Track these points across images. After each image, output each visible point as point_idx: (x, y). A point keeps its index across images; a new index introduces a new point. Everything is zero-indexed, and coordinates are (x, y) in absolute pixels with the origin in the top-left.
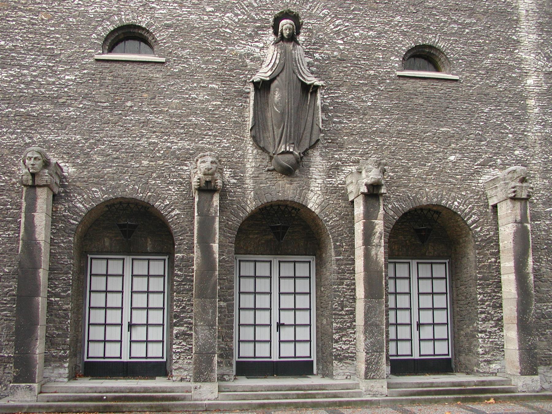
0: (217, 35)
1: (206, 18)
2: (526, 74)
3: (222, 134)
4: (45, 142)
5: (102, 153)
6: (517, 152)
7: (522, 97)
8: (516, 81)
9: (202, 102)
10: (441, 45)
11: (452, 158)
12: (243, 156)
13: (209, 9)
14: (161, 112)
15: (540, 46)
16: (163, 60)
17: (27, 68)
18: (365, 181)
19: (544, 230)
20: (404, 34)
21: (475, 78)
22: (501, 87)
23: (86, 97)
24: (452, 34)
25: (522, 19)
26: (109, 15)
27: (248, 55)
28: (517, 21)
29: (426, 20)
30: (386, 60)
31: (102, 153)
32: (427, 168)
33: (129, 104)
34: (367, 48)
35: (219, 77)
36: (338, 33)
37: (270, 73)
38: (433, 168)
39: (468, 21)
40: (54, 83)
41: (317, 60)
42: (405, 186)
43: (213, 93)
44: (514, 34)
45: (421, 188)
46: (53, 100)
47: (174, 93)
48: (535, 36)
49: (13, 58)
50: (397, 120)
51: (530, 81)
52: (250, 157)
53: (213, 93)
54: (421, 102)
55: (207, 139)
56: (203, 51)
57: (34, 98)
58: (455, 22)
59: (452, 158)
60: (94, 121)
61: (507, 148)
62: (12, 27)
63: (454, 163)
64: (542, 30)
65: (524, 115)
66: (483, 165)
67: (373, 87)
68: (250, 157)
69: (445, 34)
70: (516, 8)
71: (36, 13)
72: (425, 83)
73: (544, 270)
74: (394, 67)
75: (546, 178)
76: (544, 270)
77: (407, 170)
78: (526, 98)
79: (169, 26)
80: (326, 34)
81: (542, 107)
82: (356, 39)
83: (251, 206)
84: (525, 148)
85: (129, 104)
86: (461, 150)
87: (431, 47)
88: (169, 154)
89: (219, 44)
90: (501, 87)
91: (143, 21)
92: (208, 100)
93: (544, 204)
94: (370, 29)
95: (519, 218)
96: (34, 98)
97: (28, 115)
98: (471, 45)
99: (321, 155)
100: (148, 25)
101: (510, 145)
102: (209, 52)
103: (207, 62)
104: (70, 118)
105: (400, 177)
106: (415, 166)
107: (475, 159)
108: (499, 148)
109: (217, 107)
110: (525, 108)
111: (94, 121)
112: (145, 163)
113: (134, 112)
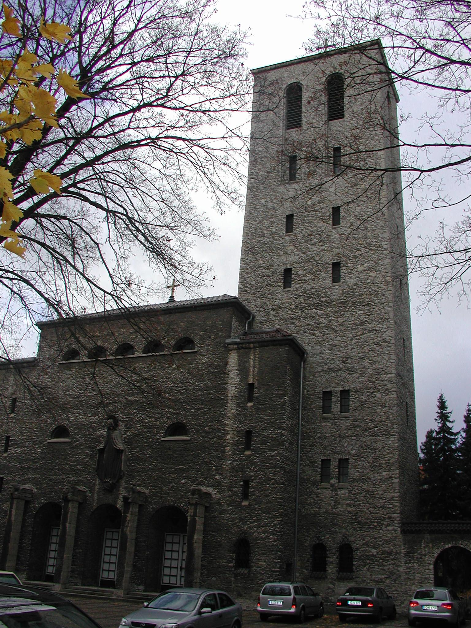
0: (91, 427)
1: (87, 419)
2: (227, 433)
4: (29, 478)
5: (46, 483)
6: (217, 477)
7: (222, 447)
8: (221, 437)
9: (82, 459)
11: (183, 481)
12: (95, 483)
13: (90, 415)
14: (68, 464)
15: (236, 416)
16: (70, 440)
19: (226, 520)
20: (168, 418)
21: (199, 438)
22: (212, 441)
23: (43, 458)
24: (191, 415)
25: (229, 401)
28: (226, 403)
29: (180, 409)
30: (158, 432)
31: (46, 483)
32: (170, 487)
33: (57, 461)
34: (150, 427)
36: (138, 421)
38: (173, 486)
39: (200, 406)
40: (33, 453)
41: (128, 436)
42: (159, 496)
44: (223, 411)
45: (166, 498)
46: (32, 460)
47: (73, 455)
48: (235, 411)
50: (159, 463)
51: (229, 437)
52: (97, 483)
54: (171, 453)
56: (86, 435)
58: (194, 408)
59: (183, 481)
60: (45, 469)
61: (213, 475)
62: (23, 430)
63: (183, 484)
64: (239, 407)
65: (223, 456)
68: (97, 483)
69: (188, 415)
70: (227, 396)
71: (31, 423)
72: (174, 443)
73: (223, 541)
74: (161, 436)
75: (230, 491)
76: (223, 541)
77: (161, 488)
78: (226, 446)
79: (74, 425)
80: (134, 422)
82: (146, 423)
83: (95, 506)
84: (221, 474)
85: (57, 461)
86: (187, 477)
87: (180, 423)
89: (91, 432)
90: (212, 441)
92: (85, 458)
93: (228, 505)
94: (153, 417)
95: (192, 514)
96: (28, 460)
97: (24, 467)
98: (200, 420)
99: (125, 482)
100: (68, 425)
101: (213, 473)
102: (86, 435)
103: (86, 440)
104: (38, 468)
105: (157, 492)
106: (165, 486)
107: (194, 482)
108: (207, 475)
110: (224, 452)
111: (45, 469)
112: (60, 487)
113: (59, 465)
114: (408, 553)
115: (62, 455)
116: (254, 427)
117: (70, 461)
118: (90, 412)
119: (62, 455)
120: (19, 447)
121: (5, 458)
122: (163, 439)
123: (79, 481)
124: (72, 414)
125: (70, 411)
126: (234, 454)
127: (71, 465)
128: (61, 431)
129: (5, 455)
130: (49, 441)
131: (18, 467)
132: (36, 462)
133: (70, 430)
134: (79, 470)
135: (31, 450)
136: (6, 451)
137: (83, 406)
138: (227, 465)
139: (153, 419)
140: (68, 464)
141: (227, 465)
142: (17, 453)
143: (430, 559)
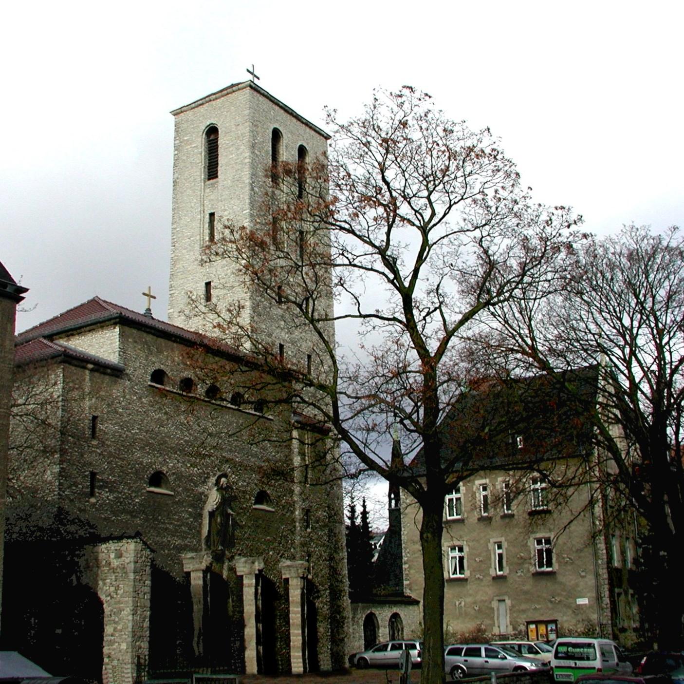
3: (193, 537)
7: (294, 521)
10: (268, 492)
14: (172, 523)
16: (172, 493)
17: (121, 493)
18: (257, 568)
26: (150, 465)
27: (203, 493)
35: (192, 506)
37: (215, 506)
43: (190, 514)
47: (176, 512)
49: (115, 487)
53: (190, 514)
55: (188, 539)
57: (124, 511)
66: (281, 557)
67: (245, 514)
71: (122, 459)
78: (295, 522)
79: (174, 474)
81: (301, 527)
82: (240, 487)
84: (294, 549)
86: (273, 549)
88: (175, 547)
91: (165, 469)
94: (245, 481)
102: (187, 490)
103: (188, 496)
109: (192, 522)
110: (295, 527)
114: (353, 618)
115: (165, 511)
116: (311, 507)
117: (174, 519)
118: (189, 461)
119: (165, 511)
120: (111, 491)
121: (94, 505)
122: (254, 507)
123: (186, 545)
124: (170, 458)
125: (167, 454)
126: (302, 530)
127: (176, 525)
128: (157, 479)
129: (93, 500)
130: (148, 489)
131: (113, 521)
132: (135, 517)
133: (171, 478)
134: (185, 532)
135: (127, 498)
136: (92, 494)
137: (180, 450)
138: (298, 539)
139: (245, 484)
140: (172, 523)
141: (298, 539)
142: (109, 499)
143: (362, 623)
